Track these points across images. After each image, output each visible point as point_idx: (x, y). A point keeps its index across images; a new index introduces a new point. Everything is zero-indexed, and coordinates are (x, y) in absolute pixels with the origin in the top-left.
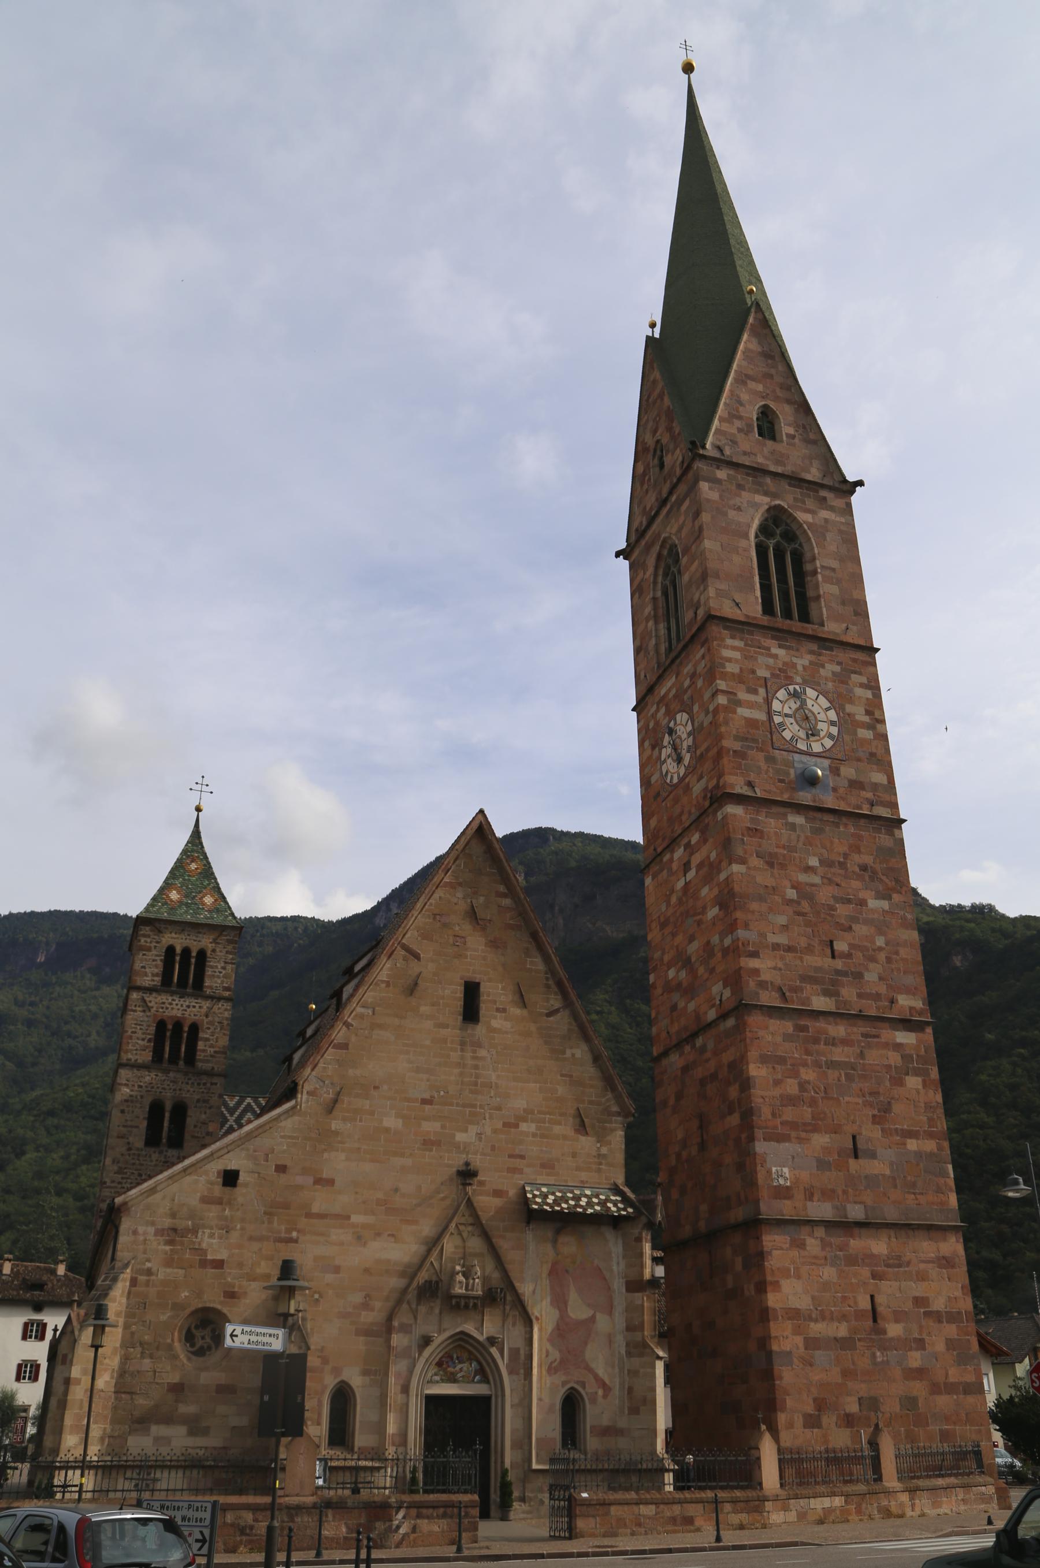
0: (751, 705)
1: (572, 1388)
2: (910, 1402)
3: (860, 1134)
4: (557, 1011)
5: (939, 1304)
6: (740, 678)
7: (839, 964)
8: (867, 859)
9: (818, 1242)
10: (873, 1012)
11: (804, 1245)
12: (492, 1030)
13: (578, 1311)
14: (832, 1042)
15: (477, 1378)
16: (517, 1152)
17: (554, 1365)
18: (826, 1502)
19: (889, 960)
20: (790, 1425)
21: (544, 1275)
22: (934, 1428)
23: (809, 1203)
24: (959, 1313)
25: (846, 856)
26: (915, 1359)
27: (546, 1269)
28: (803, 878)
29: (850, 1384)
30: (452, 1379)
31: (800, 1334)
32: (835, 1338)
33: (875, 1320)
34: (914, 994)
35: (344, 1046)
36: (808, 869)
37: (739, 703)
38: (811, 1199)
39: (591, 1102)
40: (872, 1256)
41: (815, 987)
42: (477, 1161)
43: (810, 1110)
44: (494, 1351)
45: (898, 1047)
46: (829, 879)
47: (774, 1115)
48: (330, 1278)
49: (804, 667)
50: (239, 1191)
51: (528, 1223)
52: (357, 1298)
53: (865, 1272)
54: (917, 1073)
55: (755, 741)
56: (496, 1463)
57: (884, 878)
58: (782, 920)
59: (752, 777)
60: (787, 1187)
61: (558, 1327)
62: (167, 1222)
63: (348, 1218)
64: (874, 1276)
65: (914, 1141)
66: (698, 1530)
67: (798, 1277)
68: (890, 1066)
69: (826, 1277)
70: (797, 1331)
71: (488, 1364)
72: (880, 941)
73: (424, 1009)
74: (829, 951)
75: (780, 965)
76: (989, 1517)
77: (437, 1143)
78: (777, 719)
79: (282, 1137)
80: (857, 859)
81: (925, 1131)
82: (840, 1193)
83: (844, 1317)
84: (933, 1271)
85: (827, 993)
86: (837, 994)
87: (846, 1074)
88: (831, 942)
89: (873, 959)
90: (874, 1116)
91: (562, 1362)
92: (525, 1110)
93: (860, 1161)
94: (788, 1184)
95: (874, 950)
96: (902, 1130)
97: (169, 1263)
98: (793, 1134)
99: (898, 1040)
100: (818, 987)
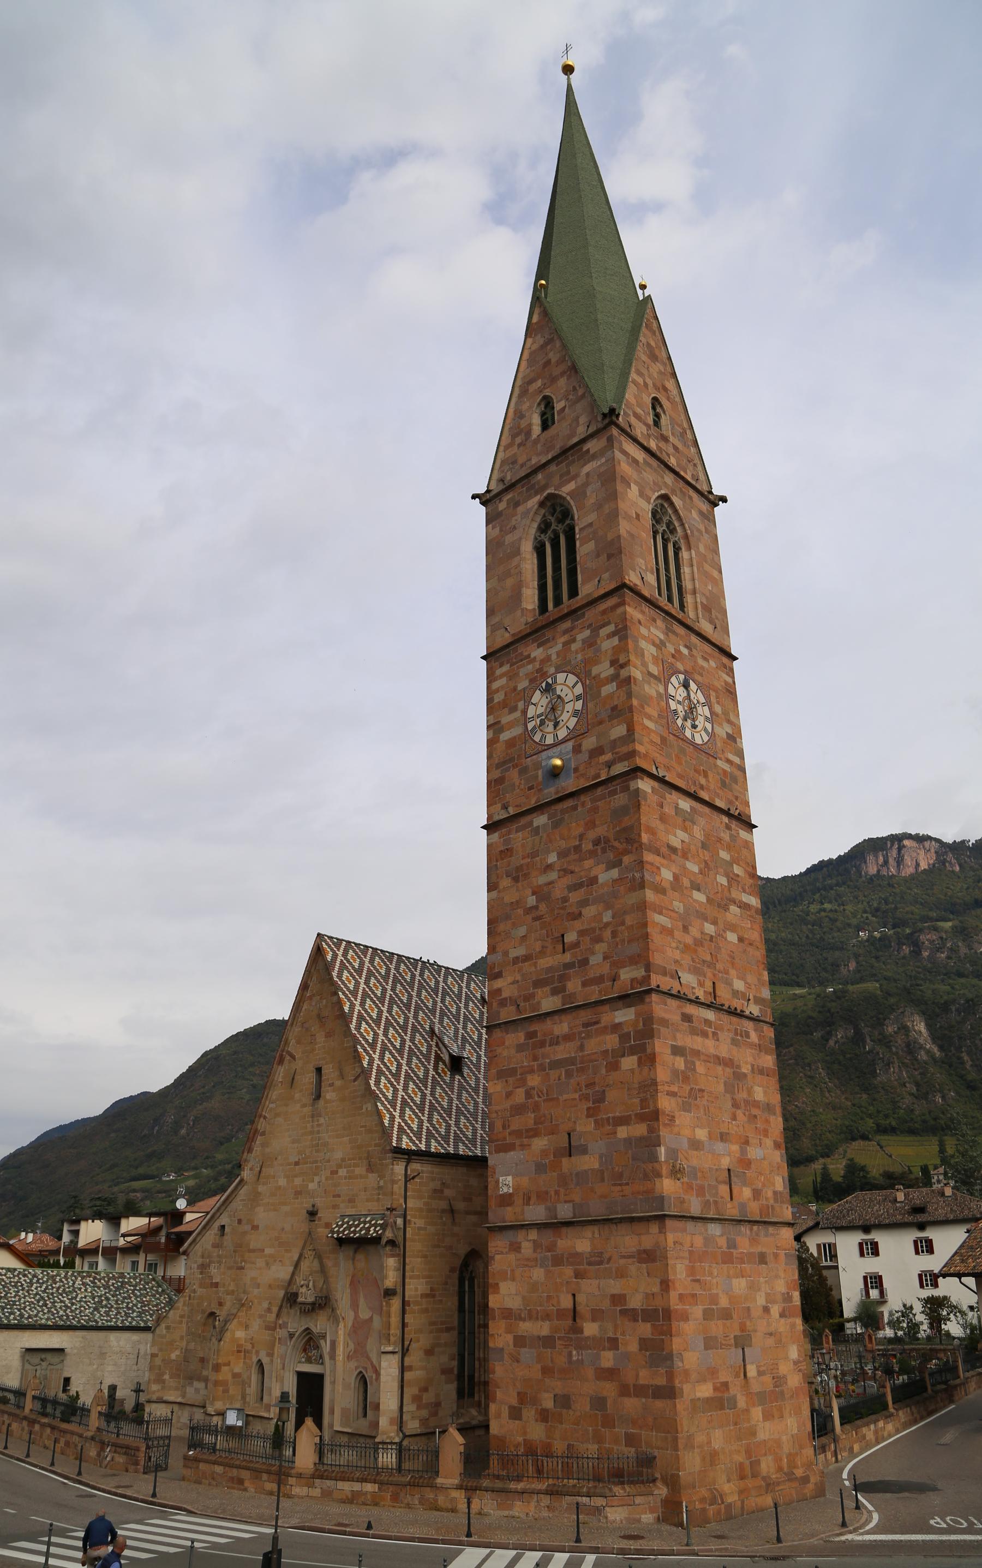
0: (511, 725)
2: (599, 1402)
3: (574, 1130)
5: (635, 1302)
7: (568, 957)
8: (600, 831)
9: (530, 1245)
11: (520, 1248)
12: (327, 1102)
13: (364, 1314)
14: (555, 1041)
18: (357, 1487)
19: (614, 934)
20: (498, 1416)
22: (620, 1430)
24: (656, 1310)
25: (581, 837)
26: (608, 1359)
27: (348, 1283)
28: (542, 880)
30: (309, 1360)
31: (510, 1332)
32: (539, 1337)
33: (575, 1320)
34: (636, 963)
35: (263, 1134)
36: (549, 867)
38: (528, 1204)
39: (376, 1145)
40: (577, 1255)
41: (545, 989)
42: (319, 1202)
44: (322, 1342)
45: (616, 1027)
47: (504, 1127)
48: (256, 1291)
49: (558, 654)
50: (225, 1237)
51: (341, 1246)
52: (265, 1305)
53: (568, 1271)
55: (512, 760)
57: (616, 844)
58: (522, 931)
60: (511, 1195)
62: (200, 1261)
64: (578, 1275)
65: (624, 1128)
66: (245, 1490)
67: (513, 1279)
68: (607, 1051)
69: (535, 1278)
70: (508, 1331)
72: (607, 917)
73: (297, 1096)
75: (519, 978)
76: (369, 1522)
78: (530, 726)
79: (241, 1200)
80: (592, 835)
81: (636, 1115)
82: (553, 1193)
83: (547, 1317)
84: (633, 1268)
85: (555, 992)
86: (563, 989)
87: (566, 1071)
88: (563, 936)
89: (599, 940)
90: (588, 1109)
92: (343, 1160)
94: (511, 1191)
95: (600, 929)
96: (614, 1118)
97: (201, 1286)
98: (518, 1142)
99: (617, 1021)
100: (547, 989)
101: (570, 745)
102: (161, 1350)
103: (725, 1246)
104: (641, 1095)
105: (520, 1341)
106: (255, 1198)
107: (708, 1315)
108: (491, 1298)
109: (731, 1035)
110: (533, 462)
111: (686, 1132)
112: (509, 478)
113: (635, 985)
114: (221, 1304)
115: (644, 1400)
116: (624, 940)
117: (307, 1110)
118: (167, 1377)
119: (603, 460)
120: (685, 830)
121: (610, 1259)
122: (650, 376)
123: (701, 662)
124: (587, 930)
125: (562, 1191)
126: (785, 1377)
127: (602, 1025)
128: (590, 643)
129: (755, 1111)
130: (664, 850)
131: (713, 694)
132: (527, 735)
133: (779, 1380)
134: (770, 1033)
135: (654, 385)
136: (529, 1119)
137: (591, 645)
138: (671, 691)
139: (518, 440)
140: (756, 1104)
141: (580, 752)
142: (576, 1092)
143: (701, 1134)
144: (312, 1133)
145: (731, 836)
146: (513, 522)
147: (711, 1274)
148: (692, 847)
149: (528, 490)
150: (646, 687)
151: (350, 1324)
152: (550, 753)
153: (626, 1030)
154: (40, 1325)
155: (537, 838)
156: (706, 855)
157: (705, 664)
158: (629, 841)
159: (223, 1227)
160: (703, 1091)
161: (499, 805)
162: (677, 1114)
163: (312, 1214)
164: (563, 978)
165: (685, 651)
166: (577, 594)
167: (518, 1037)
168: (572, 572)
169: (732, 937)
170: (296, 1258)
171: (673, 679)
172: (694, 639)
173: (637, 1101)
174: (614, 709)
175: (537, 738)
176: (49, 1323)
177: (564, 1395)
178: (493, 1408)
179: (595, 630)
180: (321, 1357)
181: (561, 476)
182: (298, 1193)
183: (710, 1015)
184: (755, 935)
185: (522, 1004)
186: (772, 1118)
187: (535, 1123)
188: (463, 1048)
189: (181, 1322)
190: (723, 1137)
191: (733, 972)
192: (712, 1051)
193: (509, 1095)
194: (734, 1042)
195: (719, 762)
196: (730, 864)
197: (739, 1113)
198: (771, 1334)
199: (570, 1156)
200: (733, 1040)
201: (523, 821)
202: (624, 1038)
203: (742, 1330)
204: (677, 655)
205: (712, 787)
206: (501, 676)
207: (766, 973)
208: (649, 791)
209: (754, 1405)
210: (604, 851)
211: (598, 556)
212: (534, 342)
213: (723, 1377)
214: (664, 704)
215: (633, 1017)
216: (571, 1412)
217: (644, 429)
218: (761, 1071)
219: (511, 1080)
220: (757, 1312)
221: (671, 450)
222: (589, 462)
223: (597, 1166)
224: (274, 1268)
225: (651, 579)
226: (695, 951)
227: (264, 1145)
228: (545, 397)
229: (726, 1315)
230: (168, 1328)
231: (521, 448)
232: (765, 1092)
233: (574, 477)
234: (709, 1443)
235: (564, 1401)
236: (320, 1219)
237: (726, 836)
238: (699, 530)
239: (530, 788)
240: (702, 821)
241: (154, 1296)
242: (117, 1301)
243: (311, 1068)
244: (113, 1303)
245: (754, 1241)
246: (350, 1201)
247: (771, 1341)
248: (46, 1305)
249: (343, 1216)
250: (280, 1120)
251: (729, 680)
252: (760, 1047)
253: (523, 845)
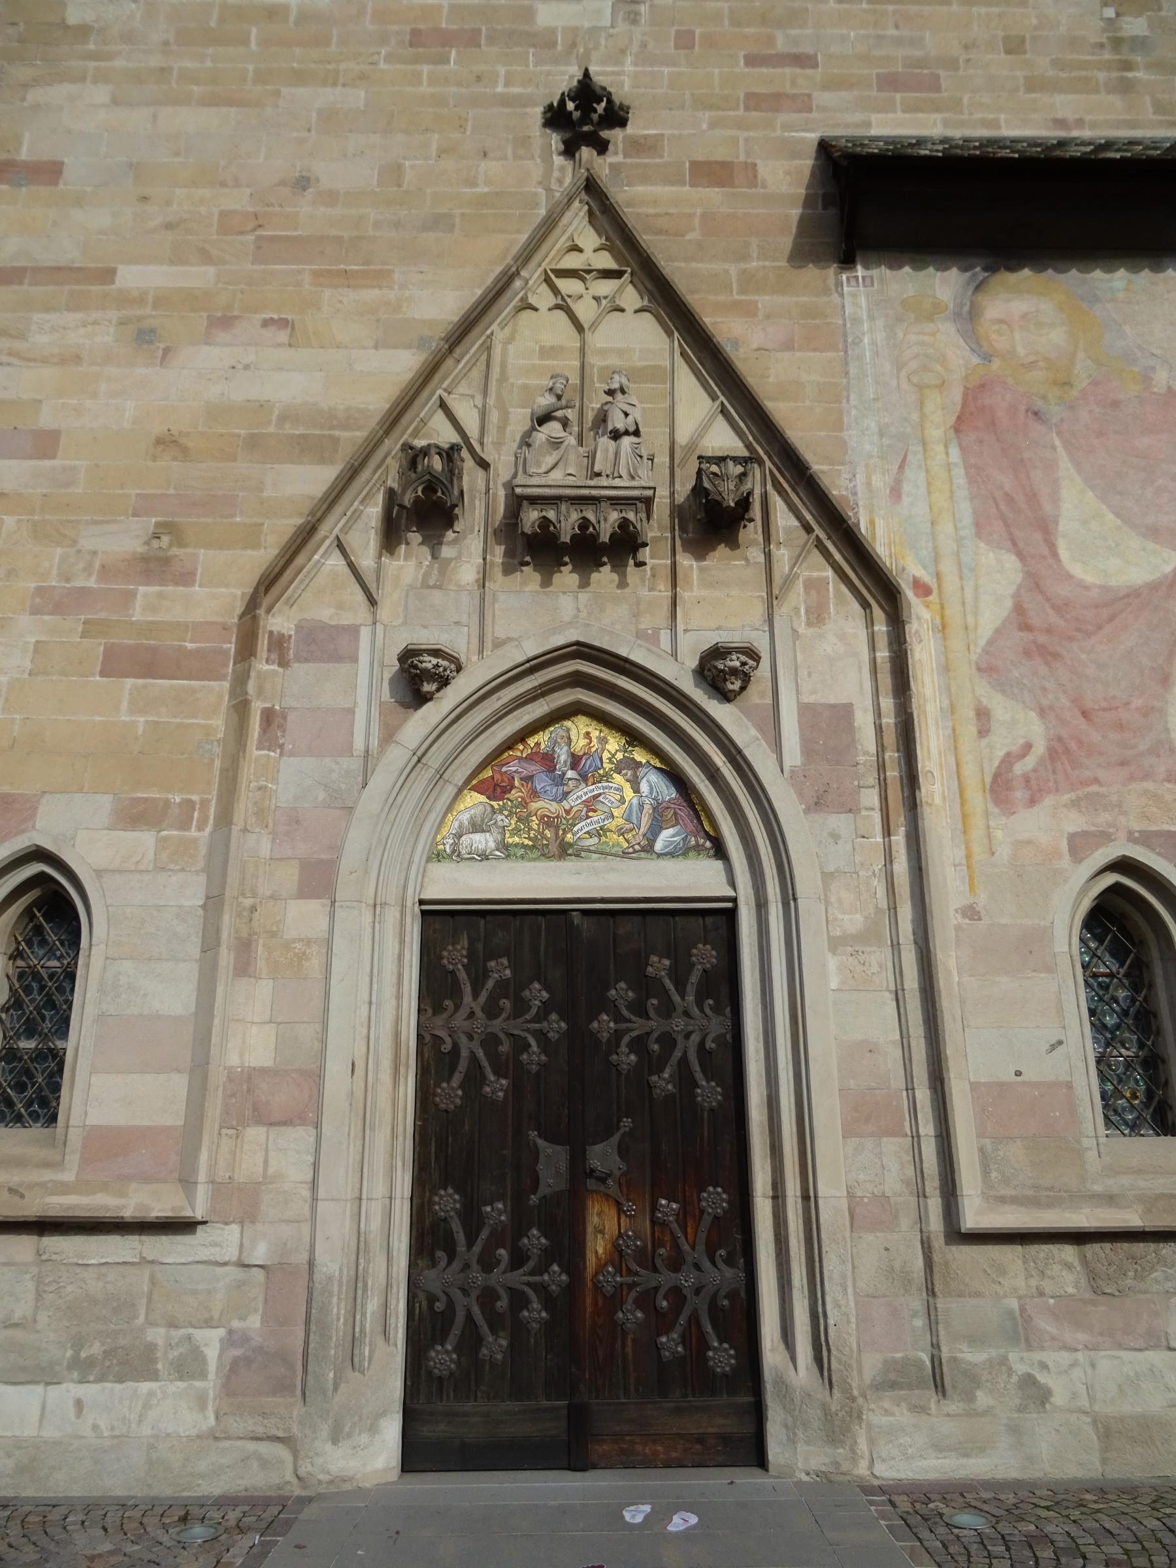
1: (1123, 865)
15: (667, 837)
16: (781, 44)
17: (1019, 768)
21: (935, 433)
52: (126, 539)
56: (778, 1197)
61: (1020, 617)
63: (109, 275)
71: (713, 775)
91: (1057, 752)
151: (990, 616)
163: (585, 117)
170: (444, 304)
246: (890, 82)
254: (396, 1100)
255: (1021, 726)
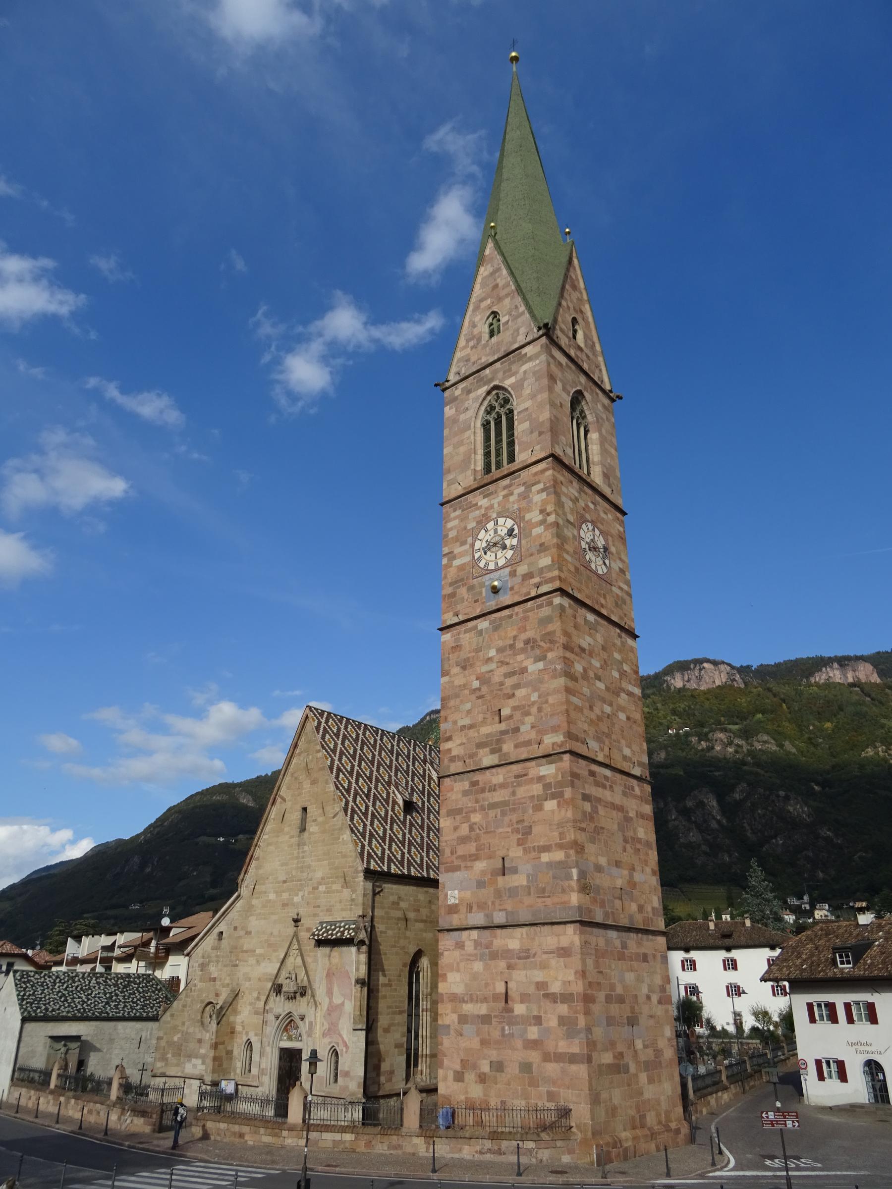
0: (462, 555)
2: (526, 1067)
4: (337, 814)
5: (556, 988)
6: (456, 539)
7: (503, 726)
8: (530, 634)
10: (523, 757)
11: (464, 946)
12: (311, 834)
14: (493, 789)
19: (540, 710)
20: (445, 1079)
22: (543, 1089)
23: (469, 915)
24: (571, 994)
25: (515, 638)
26: (533, 1032)
28: (484, 669)
29: (486, 1051)
30: (290, 1038)
31: (455, 1013)
32: (478, 1016)
33: (506, 1002)
34: (556, 731)
35: (258, 859)
36: (490, 660)
37: (454, 558)
38: (470, 912)
39: (350, 867)
40: (509, 951)
42: (303, 911)
43: (474, 844)
45: (540, 779)
46: (502, 662)
47: (452, 853)
48: (247, 984)
49: (499, 504)
52: (255, 995)
53: (502, 964)
54: (553, 796)
55: (462, 580)
57: (542, 644)
58: (468, 706)
59: (459, 607)
60: (456, 905)
62: (201, 961)
64: (510, 967)
65: (547, 854)
67: (458, 970)
68: (533, 796)
70: (454, 1012)
72: (534, 697)
73: (286, 829)
74: (497, 718)
75: (464, 741)
77: (287, 905)
78: (477, 556)
80: (524, 636)
81: (556, 844)
82: (490, 903)
83: (485, 1000)
84: (553, 962)
85: (493, 752)
86: (500, 750)
87: (501, 811)
89: (528, 714)
90: (519, 839)
92: (323, 878)
93: (506, 877)
97: (201, 980)
98: (463, 865)
99: (541, 774)
100: (487, 750)
101: (507, 570)
102: (165, 1034)
103: (620, 946)
104: (561, 830)
105: (463, 1019)
106: (249, 908)
107: (609, 999)
108: (440, 985)
109: (622, 788)
110: (483, 360)
111: (592, 859)
112: (463, 372)
113: (555, 747)
114: (217, 995)
115: (562, 1065)
116: (547, 715)
117: (295, 840)
118: (169, 1056)
119: (537, 362)
120: (590, 635)
121: (535, 954)
122: (571, 301)
123: (602, 515)
124: (518, 706)
125: (497, 902)
126: (662, 1050)
127: (530, 776)
128: (524, 496)
129: (639, 846)
130: (577, 650)
131: (610, 538)
132: (475, 562)
133: (658, 1053)
134: (648, 788)
135: (575, 309)
136: (471, 848)
137: (525, 498)
138: (582, 534)
139: (471, 344)
140: (639, 841)
141: (515, 576)
142: (509, 826)
143: (603, 861)
144: (297, 858)
145: (622, 642)
146: (466, 405)
147: (610, 967)
148: (596, 649)
149: (478, 381)
150: (566, 530)
151: (325, 1008)
152: (492, 576)
153: (548, 781)
154: (63, 1016)
155: (481, 638)
156: (604, 655)
157: (604, 516)
158: (552, 642)
159: (222, 933)
160: (603, 828)
161: (451, 613)
162: (586, 845)
163: (296, 921)
164: (499, 741)
165: (592, 506)
166: (514, 461)
167: (464, 784)
168: (511, 444)
169: (622, 716)
171: (584, 526)
172: (598, 498)
173: (556, 834)
174: (542, 545)
175: (482, 564)
176: (69, 1015)
177: (498, 1062)
178: (441, 1072)
179: (528, 486)
180: (300, 1035)
181: (504, 373)
182: (285, 905)
183: (608, 772)
184: (638, 716)
185: (467, 761)
186: (650, 852)
187: (477, 850)
188: (411, 795)
189: (183, 1011)
190: (618, 864)
191: (623, 742)
192: (609, 799)
193: (456, 828)
194: (624, 794)
195: (614, 588)
196: (621, 663)
197: (628, 846)
198: (651, 1016)
199: (504, 875)
200: (623, 791)
201: (470, 624)
202: (547, 786)
203: (632, 1013)
204: (586, 509)
205: (609, 605)
206: (455, 518)
207: (645, 744)
208: (567, 606)
209: (641, 1072)
210: (532, 648)
211: (532, 432)
212: (486, 270)
213: (620, 1048)
214: (577, 543)
215: (554, 771)
216: (503, 1075)
217: (567, 340)
218: (642, 816)
219: (458, 817)
220: (642, 999)
221: (584, 358)
222: (526, 362)
223: (525, 883)
224: (263, 965)
225: (569, 451)
226: (597, 725)
227: (257, 868)
228: (493, 312)
229: (621, 1000)
230: (172, 1015)
231: (474, 350)
232: (646, 832)
233: (514, 374)
234: (611, 1099)
235: (498, 1066)
236: (302, 925)
237: (618, 642)
238: (602, 418)
239: (476, 601)
240: (601, 630)
241: (154, 992)
242: (124, 997)
243: (299, 808)
244: (121, 998)
245: (639, 944)
246: (327, 910)
247: (651, 1022)
248: (66, 1000)
249: (321, 923)
250: (272, 848)
251: (621, 529)
252: (641, 798)
253: (469, 642)
254: (275, 1072)
255: (326, 1026)
